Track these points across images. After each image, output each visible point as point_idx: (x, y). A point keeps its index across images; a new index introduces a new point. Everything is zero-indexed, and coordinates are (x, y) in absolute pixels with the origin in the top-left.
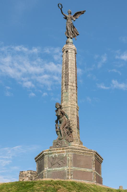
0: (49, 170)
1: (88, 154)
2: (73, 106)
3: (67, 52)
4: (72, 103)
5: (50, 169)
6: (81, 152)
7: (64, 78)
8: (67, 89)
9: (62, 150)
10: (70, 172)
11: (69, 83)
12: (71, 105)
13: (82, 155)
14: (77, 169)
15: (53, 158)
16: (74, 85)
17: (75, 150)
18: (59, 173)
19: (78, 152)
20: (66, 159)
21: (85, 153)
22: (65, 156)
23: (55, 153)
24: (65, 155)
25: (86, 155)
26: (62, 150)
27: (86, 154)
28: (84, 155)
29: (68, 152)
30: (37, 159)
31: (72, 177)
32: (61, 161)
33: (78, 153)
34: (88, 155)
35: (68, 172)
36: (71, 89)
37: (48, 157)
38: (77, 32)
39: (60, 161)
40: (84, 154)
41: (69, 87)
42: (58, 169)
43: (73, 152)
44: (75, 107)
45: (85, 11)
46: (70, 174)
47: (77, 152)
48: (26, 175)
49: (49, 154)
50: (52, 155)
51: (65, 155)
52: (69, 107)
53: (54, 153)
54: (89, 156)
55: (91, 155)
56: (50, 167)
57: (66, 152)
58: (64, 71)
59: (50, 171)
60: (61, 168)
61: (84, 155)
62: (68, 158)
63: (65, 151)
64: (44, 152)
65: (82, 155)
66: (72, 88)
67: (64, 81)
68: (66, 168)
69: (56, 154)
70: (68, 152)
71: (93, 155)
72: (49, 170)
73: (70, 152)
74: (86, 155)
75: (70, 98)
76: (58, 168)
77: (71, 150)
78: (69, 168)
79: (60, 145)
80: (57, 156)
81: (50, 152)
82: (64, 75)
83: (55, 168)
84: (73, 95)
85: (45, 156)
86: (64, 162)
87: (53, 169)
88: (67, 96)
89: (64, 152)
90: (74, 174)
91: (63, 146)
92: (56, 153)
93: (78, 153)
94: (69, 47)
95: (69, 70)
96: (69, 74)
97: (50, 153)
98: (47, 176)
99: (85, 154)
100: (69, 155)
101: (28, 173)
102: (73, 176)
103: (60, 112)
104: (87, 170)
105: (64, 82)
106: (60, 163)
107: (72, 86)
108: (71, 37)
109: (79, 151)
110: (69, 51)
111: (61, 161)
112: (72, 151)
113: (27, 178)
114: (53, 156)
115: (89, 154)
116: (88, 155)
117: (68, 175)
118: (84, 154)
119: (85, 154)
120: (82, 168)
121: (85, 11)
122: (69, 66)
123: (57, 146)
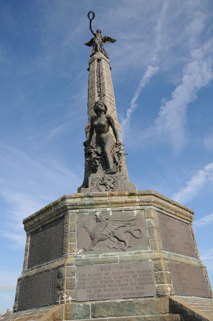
5: (88, 255)
15: (97, 220)
17: (162, 201)
18: (124, 270)
21: (179, 212)
22: (135, 215)
27: (181, 216)
29: (146, 204)
30: (31, 223)
31: (172, 285)
32: (127, 228)
35: (158, 268)
39: (121, 230)
42: (118, 255)
43: (159, 206)
46: (165, 277)
49: (84, 205)
50: (94, 210)
53: (103, 204)
54: (185, 221)
56: (87, 248)
57: (138, 204)
59: (87, 263)
60: (128, 254)
63: (137, 200)
64: (69, 201)
65: (174, 216)
67: (96, 90)
68: (146, 254)
69: (108, 209)
70: (146, 204)
72: (84, 257)
73: (152, 203)
77: (155, 198)
78: (156, 255)
79: (112, 186)
80: (111, 214)
86: (136, 234)
87: (100, 256)
89: (133, 202)
92: (106, 206)
97: (89, 202)
98: (79, 280)
100: (148, 211)
103: (106, 119)
106: (124, 237)
109: (168, 203)
111: (127, 228)
112: (158, 203)
114: (98, 214)
116: (182, 220)
123: (103, 188)
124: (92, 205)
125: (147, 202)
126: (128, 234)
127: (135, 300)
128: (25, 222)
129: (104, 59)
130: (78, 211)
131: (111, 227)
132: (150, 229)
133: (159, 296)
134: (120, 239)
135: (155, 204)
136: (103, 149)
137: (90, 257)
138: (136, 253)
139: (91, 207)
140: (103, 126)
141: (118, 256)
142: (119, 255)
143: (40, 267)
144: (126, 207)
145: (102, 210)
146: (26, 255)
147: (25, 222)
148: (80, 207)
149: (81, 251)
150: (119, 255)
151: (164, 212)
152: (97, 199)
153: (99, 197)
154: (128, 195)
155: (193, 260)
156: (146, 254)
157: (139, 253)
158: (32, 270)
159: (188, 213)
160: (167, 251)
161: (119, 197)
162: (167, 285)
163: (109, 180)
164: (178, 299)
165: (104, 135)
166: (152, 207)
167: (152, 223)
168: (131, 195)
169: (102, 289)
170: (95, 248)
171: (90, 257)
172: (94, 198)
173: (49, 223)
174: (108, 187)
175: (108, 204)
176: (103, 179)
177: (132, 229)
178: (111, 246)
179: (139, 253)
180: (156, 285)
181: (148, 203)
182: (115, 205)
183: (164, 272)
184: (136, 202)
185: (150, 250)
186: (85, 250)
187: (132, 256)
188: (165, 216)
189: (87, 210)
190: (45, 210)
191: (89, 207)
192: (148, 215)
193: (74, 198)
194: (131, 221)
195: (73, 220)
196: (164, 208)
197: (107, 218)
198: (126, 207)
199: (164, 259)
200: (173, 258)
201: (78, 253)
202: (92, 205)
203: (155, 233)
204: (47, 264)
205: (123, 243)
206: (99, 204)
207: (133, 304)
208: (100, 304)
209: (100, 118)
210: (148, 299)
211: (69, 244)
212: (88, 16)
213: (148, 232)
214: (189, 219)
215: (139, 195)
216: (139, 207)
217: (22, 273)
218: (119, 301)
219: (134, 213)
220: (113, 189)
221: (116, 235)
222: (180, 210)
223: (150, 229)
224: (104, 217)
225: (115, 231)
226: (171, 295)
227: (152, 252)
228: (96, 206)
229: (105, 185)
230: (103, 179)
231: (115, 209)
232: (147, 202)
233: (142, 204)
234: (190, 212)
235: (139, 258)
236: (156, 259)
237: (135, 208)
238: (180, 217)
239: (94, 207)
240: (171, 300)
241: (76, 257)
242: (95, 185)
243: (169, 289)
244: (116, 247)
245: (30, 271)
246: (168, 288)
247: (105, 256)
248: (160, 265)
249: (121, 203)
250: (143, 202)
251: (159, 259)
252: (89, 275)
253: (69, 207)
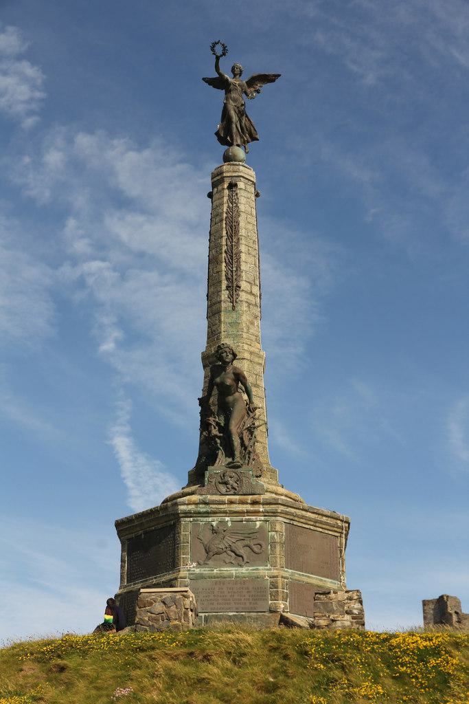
0: (197, 571)
2: (256, 360)
3: (232, 186)
4: (252, 349)
5: (202, 569)
7: (224, 264)
8: (233, 299)
9: (249, 507)
10: (280, 585)
11: (244, 285)
12: (251, 353)
13: (312, 527)
14: (299, 576)
15: (214, 531)
16: (256, 290)
17: (293, 510)
20: (265, 537)
21: (321, 522)
23: (221, 515)
24: (258, 523)
25: (321, 530)
26: (249, 507)
27: (324, 526)
28: (315, 528)
31: (288, 603)
33: (302, 520)
34: (326, 532)
35: (274, 585)
36: (249, 304)
37: (196, 525)
38: (253, 131)
39: (239, 543)
40: (317, 525)
41: (243, 296)
42: (234, 571)
43: (288, 517)
44: (260, 362)
45: (279, 75)
46: (281, 595)
47: (297, 516)
48: (341, 604)
50: (210, 519)
51: (258, 523)
52: (245, 361)
53: (221, 512)
54: (330, 533)
55: (336, 529)
56: (200, 561)
57: (262, 514)
58: (224, 243)
60: (244, 570)
61: (315, 528)
62: (273, 537)
63: (261, 510)
65: (312, 527)
66: (251, 298)
67: (224, 273)
68: (264, 571)
69: (227, 519)
70: (270, 514)
71: (340, 531)
72: (197, 571)
73: (279, 514)
74: (321, 530)
75: (245, 330)
76: (234, 569)
78: (275, 572)
79: (235, 485)
81: (202, 508)
82: (224, 255)
83: (223, 566)
84: (252, 323)
85: (185, 521)
86: (256, 549)
88: (235, 324)
89: (256, 513)
90: (291, 593)
91: (244, 490)
92: (224, 515)
93: (302, 520)
94: (240, 174)
95: (243, 241)
96: (243, 257)
97: (205, 510)
99: (320, 525)
100: (273, 524)
101: (350, 599)
102: (291, 600)
104: (325, 581)
105: (224, 277)
106: (242, 551)
107: (251, 293)
108: (239, 142)
109: (304, 513)
110: (241, 185)
112: (287, 513)
113: (347, 617)
115: (331, 528)
116: (326, 532)
117: (275, 597)
118: (317, 525)
119: (320, 525)
120: (312, 574)
121: (279, 75)
122: (242, 232)
123: (223, 489)
124: (207, 514)
125: (272, 513)
126: (252, 546)
127: (247, 614)
128: (119, 525)
129: (243, 177)
130: (191, 519)
131: (229, 540)
132: (273, 544)
133: (271, 611)
134: (238, 553)
135: (282, 515)
136: (227, 421)
137: (204, 571)
138: (253, 570)
139: (207, 515)
140: (229, 387)
141: (234, 572)
142: (235, 570)
143: (146, 581)
144: (247, 517)
145: (220, 519)
146: (122, 567)
147: (119, 525)
148: (195, 515)
149: (195, 564)
150: (235, 570)
151: (295, 523)
152: (214, 506)
153: (216, 504)
154: (251, 504)
155: (331, 582)
156: (264, 571)
157: (257, 569)
158: (135, 584)
159: (339, 522)
160: (291, 569)
161: (241, 506)
162: (280, 602)
163: (231, 477)
164: (288, 615)
165: (230, 398)
166: (278, 518)
167: (275, 537)
168: (254, 503)
169: (216, 603)
170: (210, 562)
171: (204, 571)
172: (211, 506)
173: (155, 530)
174: (230, 486)
175: (227, 513)
176: (224, 476)
177: (252, 543)
178: (227, 561)
179: (257, 569)
180: (270, 602)
181: (275, 514)
182: (236, 515)
183: (280, 590)
184: (259, 512)
185: (269, 567)
186: (199, 564)
187: (249, 573)
188: (296, 529)
189: (202, 519)
190: (149, 514)
191: (205, 515)
192: (272, 528)
193: (187, 504)
194: (252, 534)
195: (186, 529)
196: (296, 519)
197: (225, 529)
198: (247, 517)
199: (282, 577)
200: (296, 577)
201: (191, 566)
202: (207, 514)
203: (278, 548)
204: (155, 578)
205: (241, 558)
206: (217, 513)
207: (245, 617)
208: (213, 616)
209: (224, 373)
210: (260, 614)
211: (182, 556)
212: (213, 48)
213: (269, 547)
214: (338, 530)
215: (263, 504)
216: (263, 518)
217: (120, 589)
218: (231, 614)
219: (256, 525)
220: (236, 490)
221: (234, 549)
222: (324, 519)
223: (273, 544)
224: (221, 528)
225: (233, 545)
226: (284, 612)
227: (270, 569)
228: (212, 515)
229: (226, 483)
230: (224, 476)
231: (235, 519)
232: (272, 513)
233: (266, 513)
234: (342, 521)
235: (255, 575)
236: (274, 577)
237: (258, 518)
238: (322, 528)
239: (210, 515)
240: (282, 616)
241: (189, 570)
242: (213, 483)
243: (282, 606)
244: (233, 562)
245: (132, 586)
246: (281, 605)
247: (220, 571)
248: (277, 582)
249: (241, 513)
250: (268, 512)
251: (277, 577)
252: (203, 589)
253: (181, 515)
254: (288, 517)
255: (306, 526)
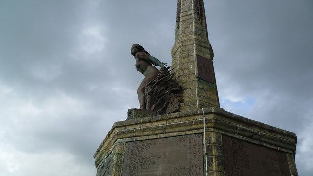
1: (182, 128)
6: (156, 129)
13: (162, 136)
17: (131, 128)
19: (145, 130)
21: (171, 126)
27: (177, 129)
28: (167, 135)
33: (146, 133)
34: (184, 133)
40: (167, 131)
43: (129, 135)
45: (138, 50)
47: (138, 131)
61: (167, 135)
65: (162, 136)
93: (146, 133)
112: (124, 133)
115: (188, 128)
116: (184, 133)
118: (167, 131)
119: (172, 130)
121: (138, 50)
135: (120, 137)
254: (129, 135)
255: (155, 137)
